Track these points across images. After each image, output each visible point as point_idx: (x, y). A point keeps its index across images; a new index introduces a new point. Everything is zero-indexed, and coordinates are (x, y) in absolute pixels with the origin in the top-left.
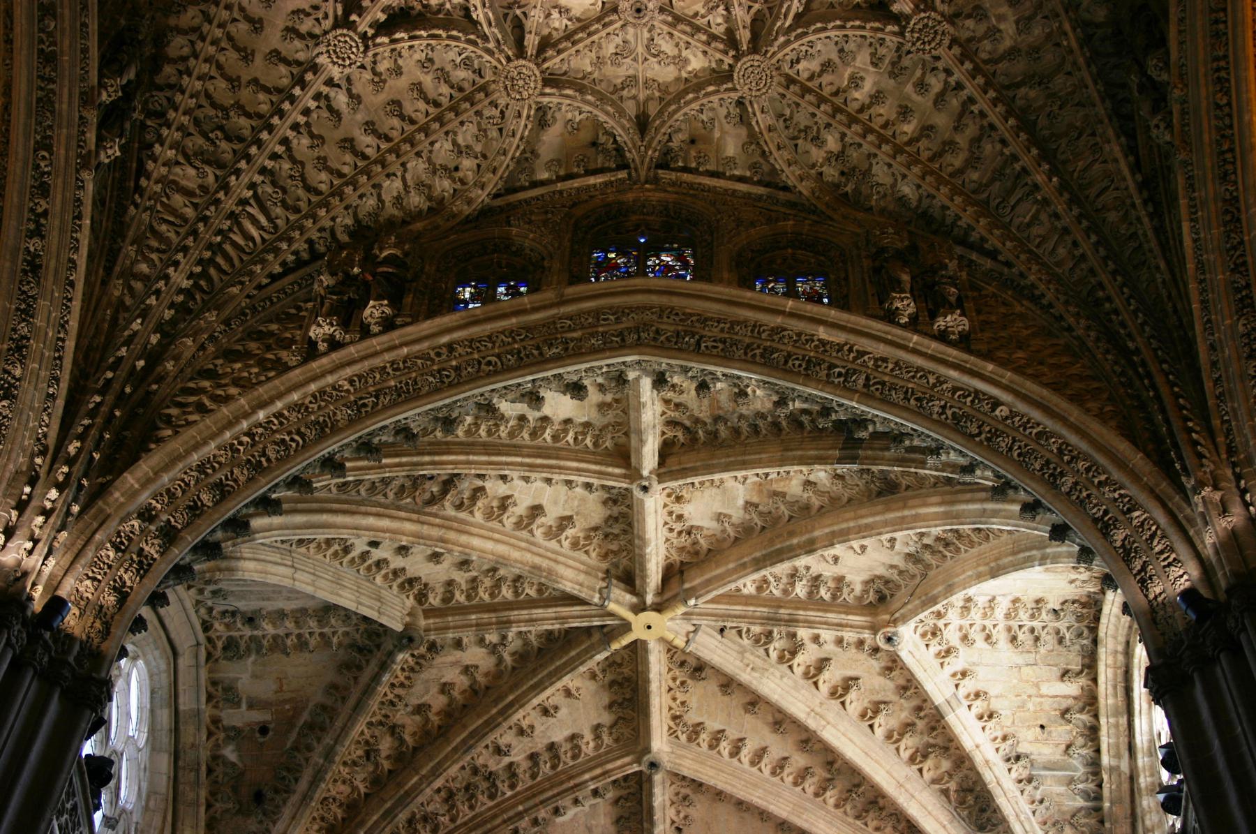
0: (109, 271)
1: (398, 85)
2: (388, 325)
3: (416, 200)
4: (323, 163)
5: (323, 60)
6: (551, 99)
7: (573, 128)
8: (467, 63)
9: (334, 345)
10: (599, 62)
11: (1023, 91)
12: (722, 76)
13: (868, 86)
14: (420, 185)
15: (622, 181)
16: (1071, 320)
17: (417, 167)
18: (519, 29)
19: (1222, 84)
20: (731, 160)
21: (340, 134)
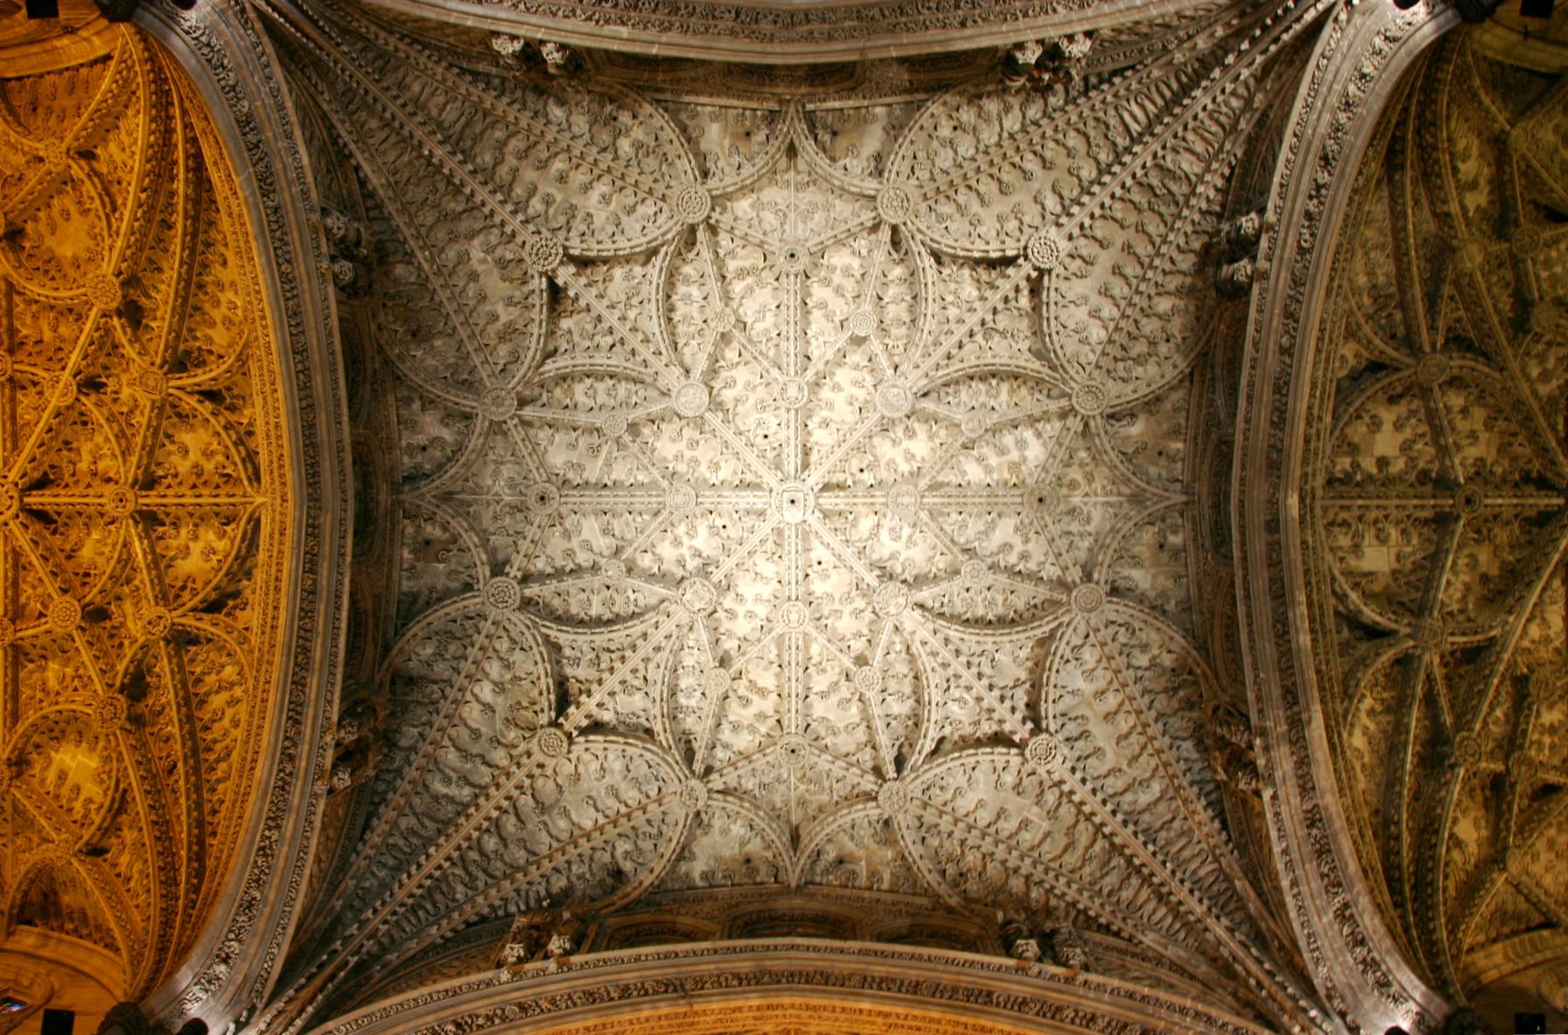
0: (1265, 115)
1: (1001, 206)
2: (1020, 46)
3: (992, 106)
4: (1070, 153)
5: (1064, 246)
6: (870, 186)
7: (851, 150)
8: (941, 218)
9: (1071, 38)
10: (828, 208)
11: (460, 208)
12: (720, 200)
13: (594, 196)
14: (988, 120)
15: (810, 102)
16: (401, 46)
17: (989, 136)
18: (895, 243)
19: (287, 279)
20: (714, 118)
21: (1055, 174)
